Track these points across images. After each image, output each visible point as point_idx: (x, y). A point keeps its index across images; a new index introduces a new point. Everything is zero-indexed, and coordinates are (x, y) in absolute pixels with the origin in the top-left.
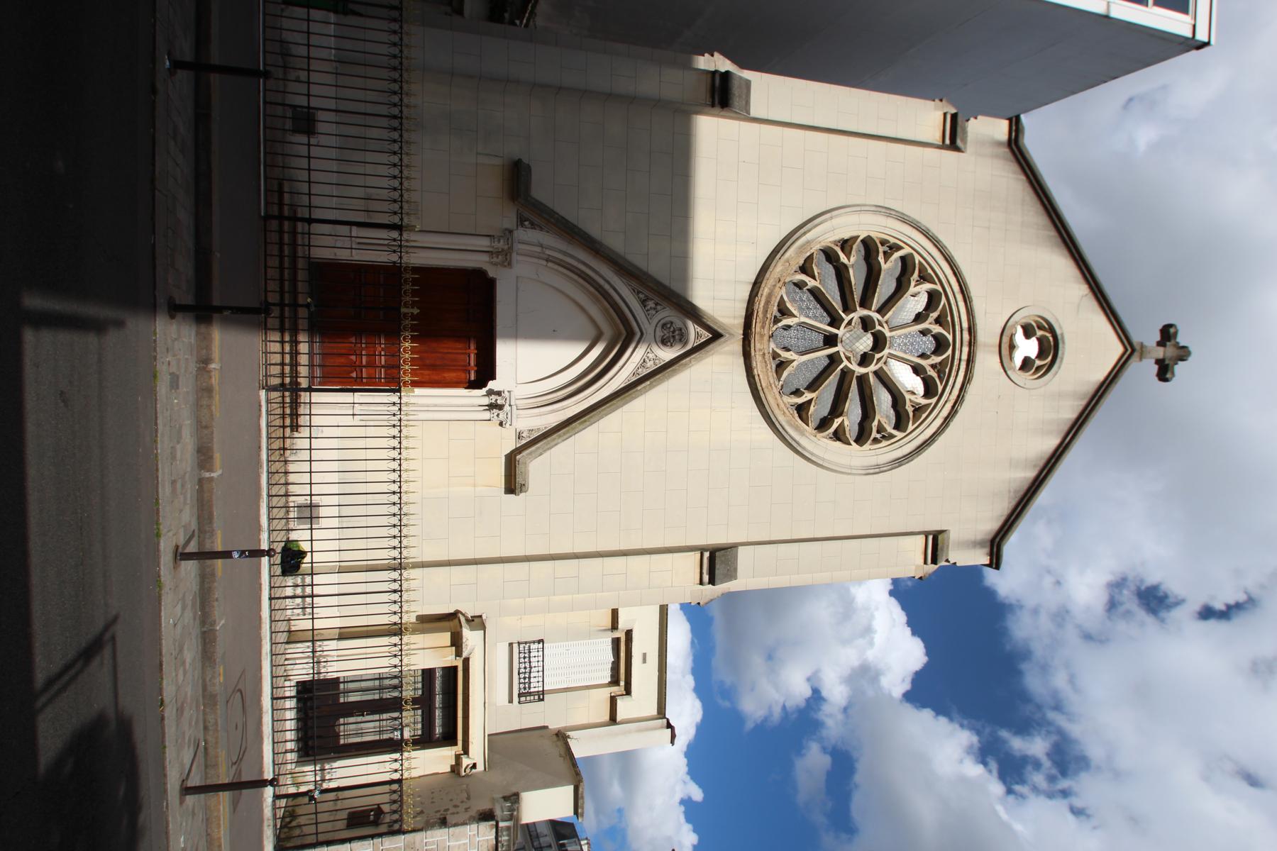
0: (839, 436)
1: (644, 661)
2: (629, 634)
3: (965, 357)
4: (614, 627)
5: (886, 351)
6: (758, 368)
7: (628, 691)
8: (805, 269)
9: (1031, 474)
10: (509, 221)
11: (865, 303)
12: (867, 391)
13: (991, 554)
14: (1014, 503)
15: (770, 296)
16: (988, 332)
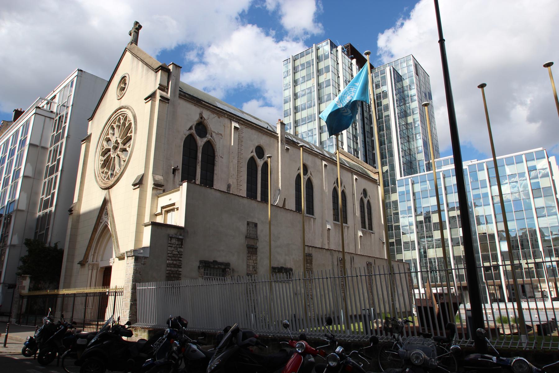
0: (129, 147)
1: (170, 199)
2: (163, 208)
3: (119, 111)
4: (161, 214)
5: (118, 139)
6: (113, 182)
7: (174, 204)
8: (103, 173)
9: (145, 66)
10: (87, 265)
11: (109, 150)
12: (125, 141)
13: (158, 71)
14: (150, 70)
15: (105, 184)
16: (117, 105)
